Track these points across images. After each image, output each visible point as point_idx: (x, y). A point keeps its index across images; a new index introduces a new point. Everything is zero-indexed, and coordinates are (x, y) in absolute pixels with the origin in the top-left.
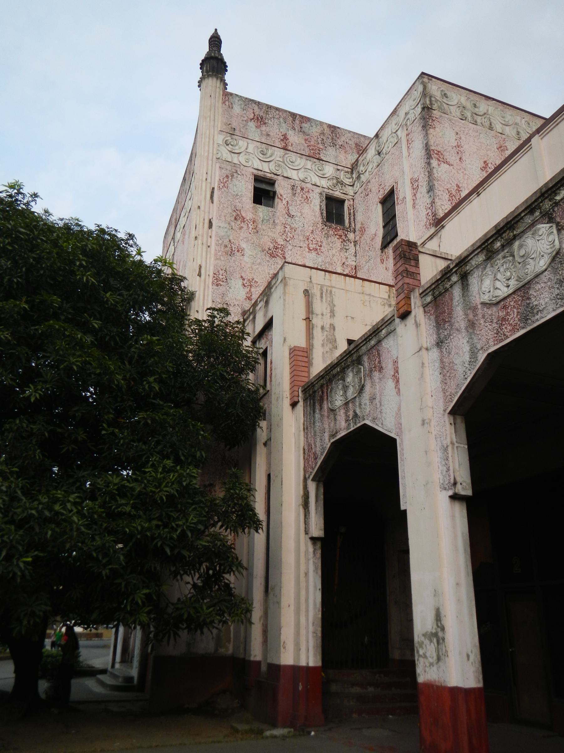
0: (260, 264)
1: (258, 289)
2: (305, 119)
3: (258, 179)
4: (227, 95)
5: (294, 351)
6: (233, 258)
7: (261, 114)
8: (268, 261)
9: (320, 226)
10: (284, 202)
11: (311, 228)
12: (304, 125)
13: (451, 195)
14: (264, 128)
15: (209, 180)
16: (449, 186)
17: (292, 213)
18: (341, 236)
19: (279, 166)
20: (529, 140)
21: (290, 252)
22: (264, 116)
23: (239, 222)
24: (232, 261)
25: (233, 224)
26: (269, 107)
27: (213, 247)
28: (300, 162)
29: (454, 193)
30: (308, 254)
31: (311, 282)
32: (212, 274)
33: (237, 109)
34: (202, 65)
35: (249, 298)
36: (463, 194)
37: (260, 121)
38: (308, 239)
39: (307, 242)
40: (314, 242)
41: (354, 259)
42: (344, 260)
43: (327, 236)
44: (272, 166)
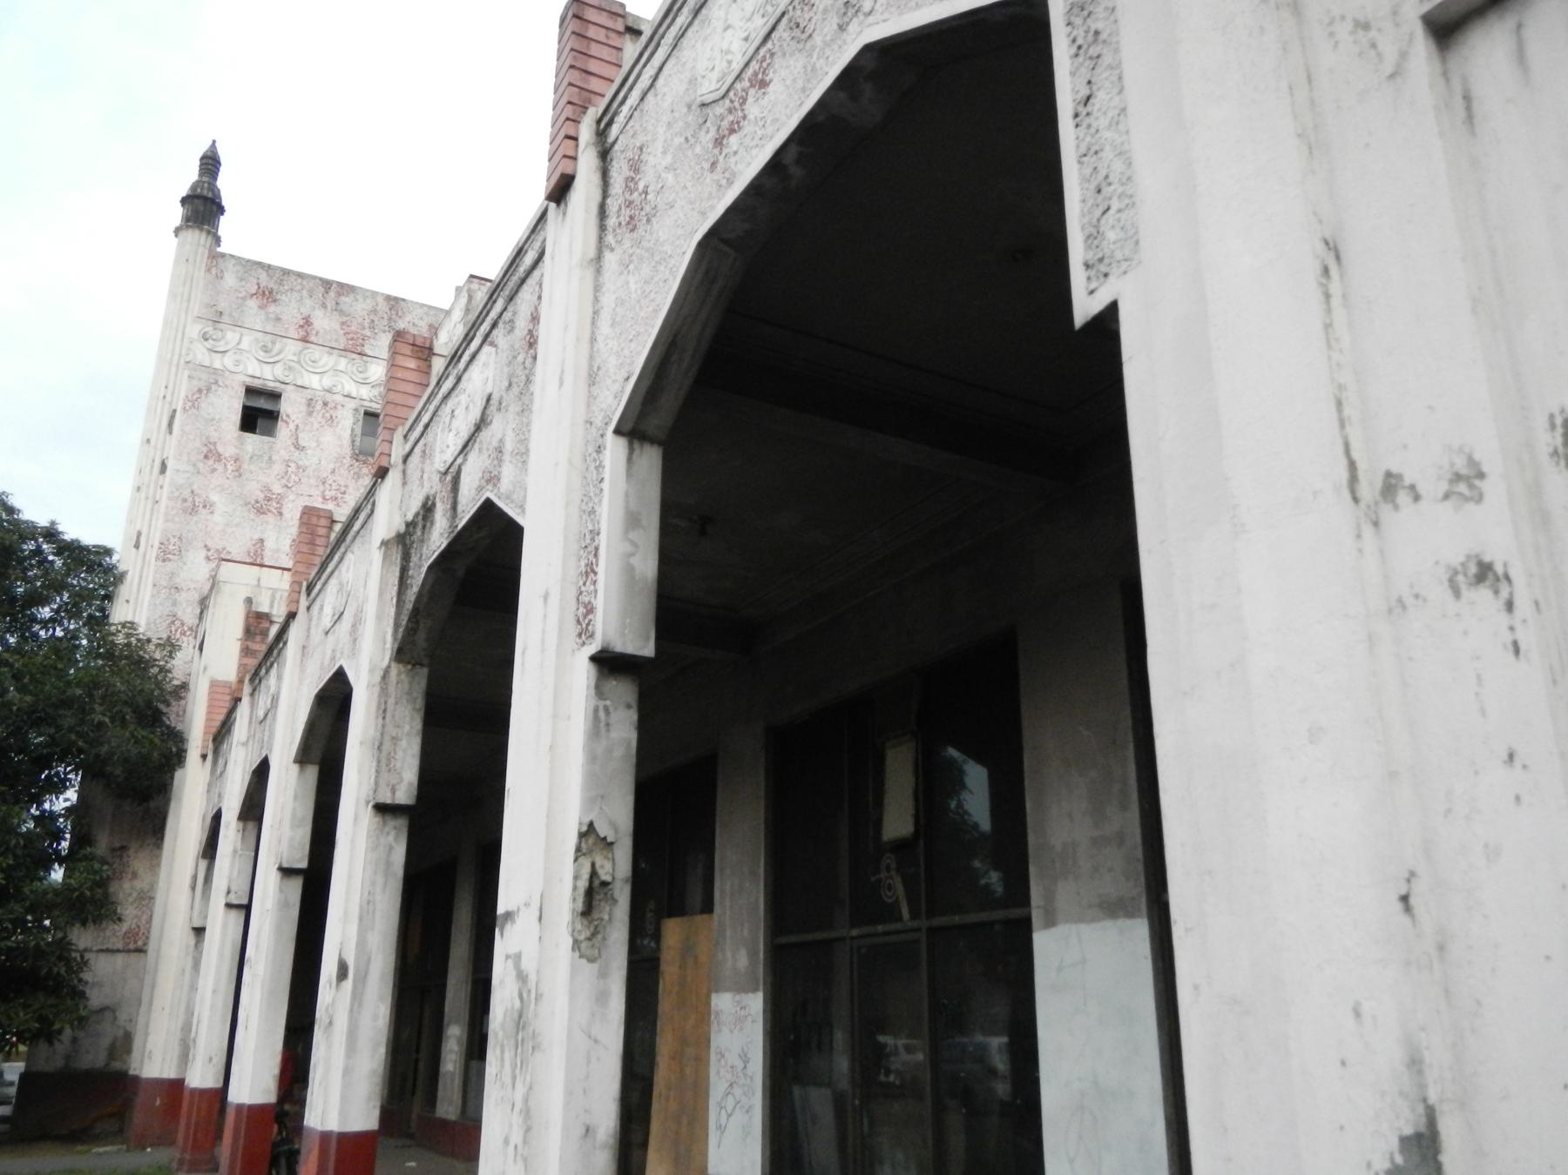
0: (237, 525)
2: (345, 289)
3: (251, 391)
4: (215, 257)
7: (271, 285)
9: (348, 461)
10: (292, 426)
11: (332, 466)
12: (343, 299)
14: (272, 308)
15: (168, 398)
17: (302, 443)
19: (290, 368)
22: (276, 287)
23: (211, 462)
25: (201, 465)
26: (286, 272)
27: (164, 502)
28: (327, 360)
31: (258, 585)
32: (157, 544)
33: (230, 280)
34: (184, 201)
37: (267, 296)
44: (279, 371)
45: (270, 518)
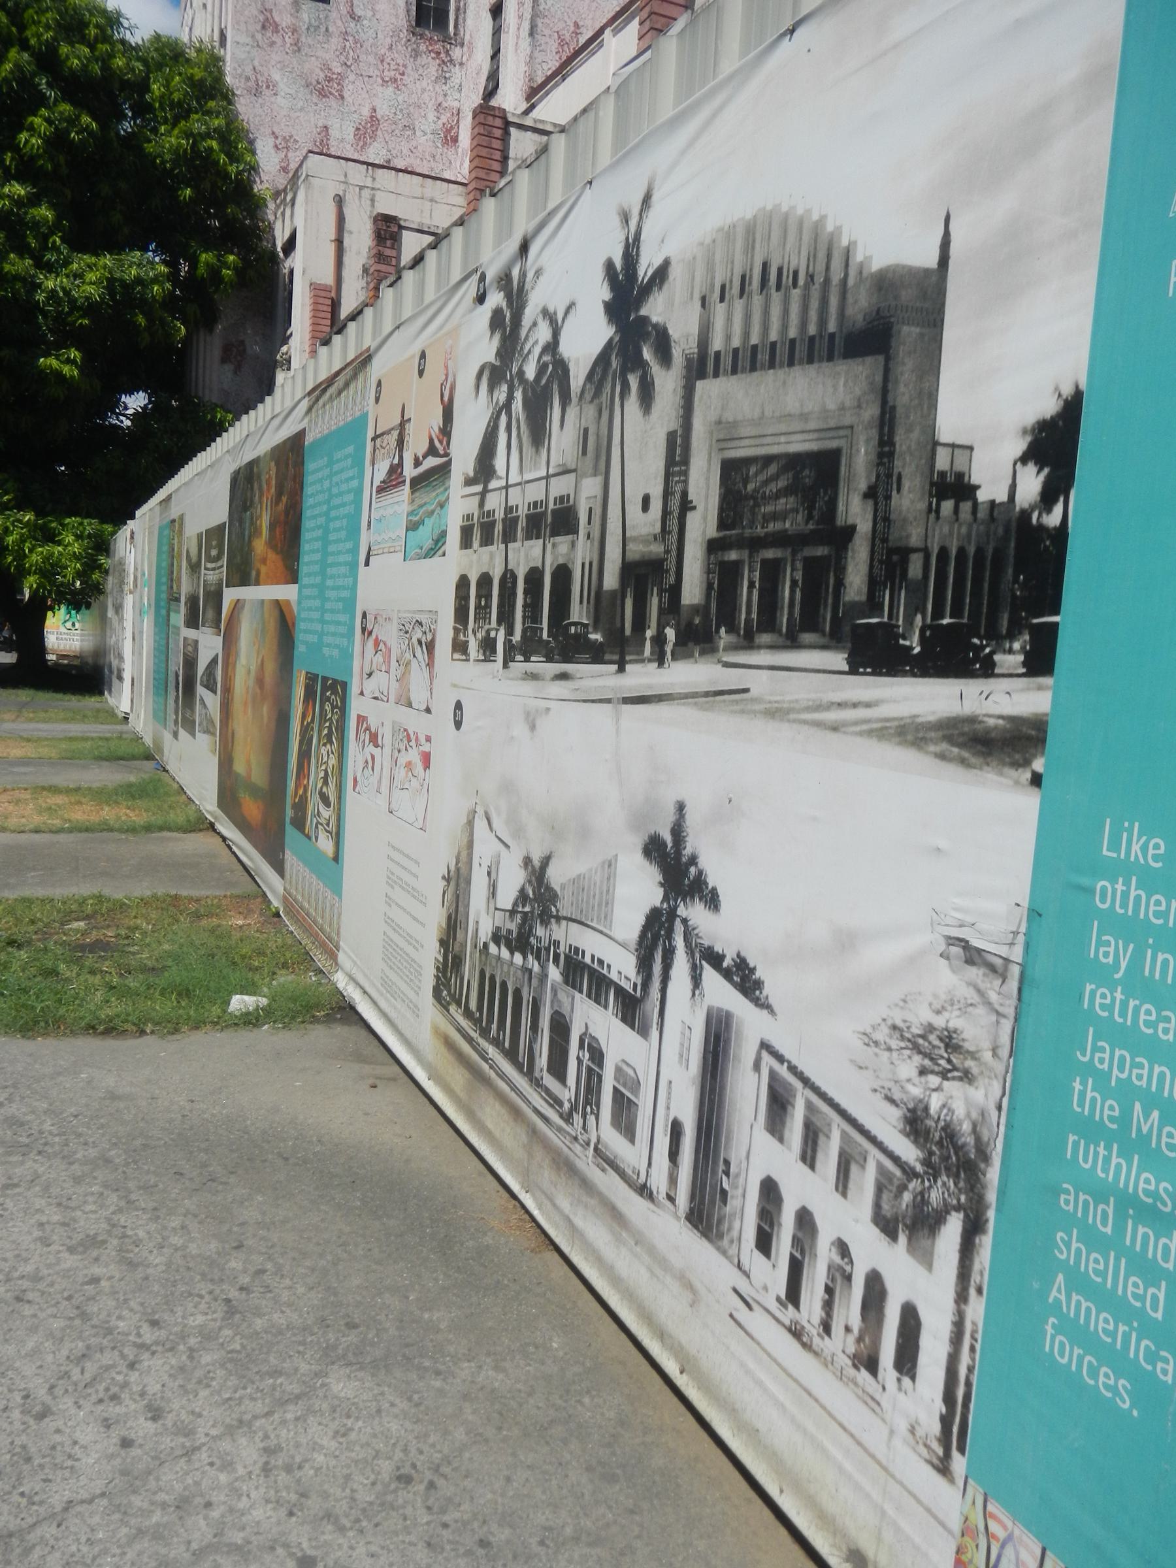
1: (298, 153)
5: (317, 289)
6: (260, 100)
8: (316, 104)
9: (404, 34)
11: (389, 40)
13: (562, 43)
16: (561, 25)
18: (438, 53)
20: (601, 32)
21: (351, 87)
23: (269, 34)
24: (258, 105)
25: (259, 36)
29: (567, 37)
30: (380, 89)
35: (285, 170)
36: (582, 40)
38: (382, 61)
39: (381, 67)
40: (393, 67)
41: (457, 96)
42: (440, 99)
43: (416, 54)
45: (332, 102)
